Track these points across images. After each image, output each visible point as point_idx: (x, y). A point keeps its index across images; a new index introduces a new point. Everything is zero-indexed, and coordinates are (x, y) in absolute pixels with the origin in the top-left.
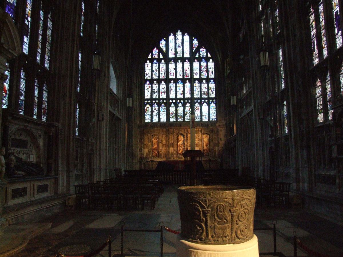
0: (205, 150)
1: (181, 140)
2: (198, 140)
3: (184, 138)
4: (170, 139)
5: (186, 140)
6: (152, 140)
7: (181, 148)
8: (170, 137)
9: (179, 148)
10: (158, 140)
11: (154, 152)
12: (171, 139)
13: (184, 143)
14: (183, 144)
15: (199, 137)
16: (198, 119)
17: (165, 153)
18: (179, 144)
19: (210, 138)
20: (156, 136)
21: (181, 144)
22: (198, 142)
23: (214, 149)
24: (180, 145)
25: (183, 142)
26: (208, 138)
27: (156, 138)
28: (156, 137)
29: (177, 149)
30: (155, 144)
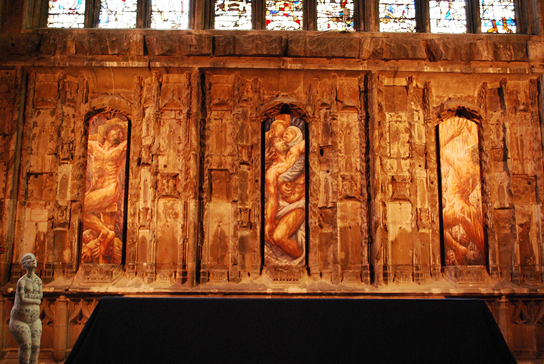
0: (456, 222)
1: (287, 151)
2: (405, 151)
3: (306, 138)
4: (211, 142)
5: (322, 152)
6: (85, 145)
7: (286, 206)
8: (212, 125)
9: (271, 203)
10: (125, 143)
11: (96, 233)
12: (221, 143)
13: (307, 171)
14: (302, 181)
15: (409, 130)
16: (403, 19)
17: (174, 240)
18: (270, 175)
19: (486, 144)
20: (114, 121)
21: (289, 175)
22: (406, 164)
23: (520, 220)
24: (278, 187)
25: (300, 167)
26: (473, 141)
27: (113, 132)
28: (112, 127)
29: (257, 211)
30: (102, 173)
